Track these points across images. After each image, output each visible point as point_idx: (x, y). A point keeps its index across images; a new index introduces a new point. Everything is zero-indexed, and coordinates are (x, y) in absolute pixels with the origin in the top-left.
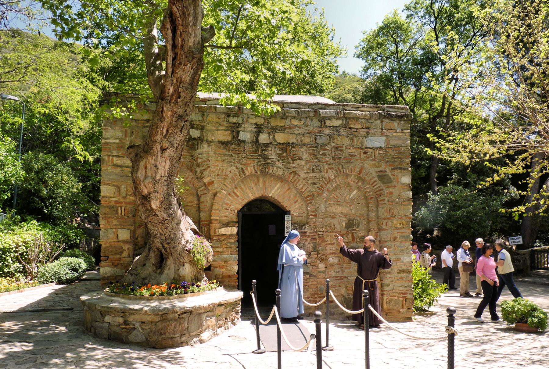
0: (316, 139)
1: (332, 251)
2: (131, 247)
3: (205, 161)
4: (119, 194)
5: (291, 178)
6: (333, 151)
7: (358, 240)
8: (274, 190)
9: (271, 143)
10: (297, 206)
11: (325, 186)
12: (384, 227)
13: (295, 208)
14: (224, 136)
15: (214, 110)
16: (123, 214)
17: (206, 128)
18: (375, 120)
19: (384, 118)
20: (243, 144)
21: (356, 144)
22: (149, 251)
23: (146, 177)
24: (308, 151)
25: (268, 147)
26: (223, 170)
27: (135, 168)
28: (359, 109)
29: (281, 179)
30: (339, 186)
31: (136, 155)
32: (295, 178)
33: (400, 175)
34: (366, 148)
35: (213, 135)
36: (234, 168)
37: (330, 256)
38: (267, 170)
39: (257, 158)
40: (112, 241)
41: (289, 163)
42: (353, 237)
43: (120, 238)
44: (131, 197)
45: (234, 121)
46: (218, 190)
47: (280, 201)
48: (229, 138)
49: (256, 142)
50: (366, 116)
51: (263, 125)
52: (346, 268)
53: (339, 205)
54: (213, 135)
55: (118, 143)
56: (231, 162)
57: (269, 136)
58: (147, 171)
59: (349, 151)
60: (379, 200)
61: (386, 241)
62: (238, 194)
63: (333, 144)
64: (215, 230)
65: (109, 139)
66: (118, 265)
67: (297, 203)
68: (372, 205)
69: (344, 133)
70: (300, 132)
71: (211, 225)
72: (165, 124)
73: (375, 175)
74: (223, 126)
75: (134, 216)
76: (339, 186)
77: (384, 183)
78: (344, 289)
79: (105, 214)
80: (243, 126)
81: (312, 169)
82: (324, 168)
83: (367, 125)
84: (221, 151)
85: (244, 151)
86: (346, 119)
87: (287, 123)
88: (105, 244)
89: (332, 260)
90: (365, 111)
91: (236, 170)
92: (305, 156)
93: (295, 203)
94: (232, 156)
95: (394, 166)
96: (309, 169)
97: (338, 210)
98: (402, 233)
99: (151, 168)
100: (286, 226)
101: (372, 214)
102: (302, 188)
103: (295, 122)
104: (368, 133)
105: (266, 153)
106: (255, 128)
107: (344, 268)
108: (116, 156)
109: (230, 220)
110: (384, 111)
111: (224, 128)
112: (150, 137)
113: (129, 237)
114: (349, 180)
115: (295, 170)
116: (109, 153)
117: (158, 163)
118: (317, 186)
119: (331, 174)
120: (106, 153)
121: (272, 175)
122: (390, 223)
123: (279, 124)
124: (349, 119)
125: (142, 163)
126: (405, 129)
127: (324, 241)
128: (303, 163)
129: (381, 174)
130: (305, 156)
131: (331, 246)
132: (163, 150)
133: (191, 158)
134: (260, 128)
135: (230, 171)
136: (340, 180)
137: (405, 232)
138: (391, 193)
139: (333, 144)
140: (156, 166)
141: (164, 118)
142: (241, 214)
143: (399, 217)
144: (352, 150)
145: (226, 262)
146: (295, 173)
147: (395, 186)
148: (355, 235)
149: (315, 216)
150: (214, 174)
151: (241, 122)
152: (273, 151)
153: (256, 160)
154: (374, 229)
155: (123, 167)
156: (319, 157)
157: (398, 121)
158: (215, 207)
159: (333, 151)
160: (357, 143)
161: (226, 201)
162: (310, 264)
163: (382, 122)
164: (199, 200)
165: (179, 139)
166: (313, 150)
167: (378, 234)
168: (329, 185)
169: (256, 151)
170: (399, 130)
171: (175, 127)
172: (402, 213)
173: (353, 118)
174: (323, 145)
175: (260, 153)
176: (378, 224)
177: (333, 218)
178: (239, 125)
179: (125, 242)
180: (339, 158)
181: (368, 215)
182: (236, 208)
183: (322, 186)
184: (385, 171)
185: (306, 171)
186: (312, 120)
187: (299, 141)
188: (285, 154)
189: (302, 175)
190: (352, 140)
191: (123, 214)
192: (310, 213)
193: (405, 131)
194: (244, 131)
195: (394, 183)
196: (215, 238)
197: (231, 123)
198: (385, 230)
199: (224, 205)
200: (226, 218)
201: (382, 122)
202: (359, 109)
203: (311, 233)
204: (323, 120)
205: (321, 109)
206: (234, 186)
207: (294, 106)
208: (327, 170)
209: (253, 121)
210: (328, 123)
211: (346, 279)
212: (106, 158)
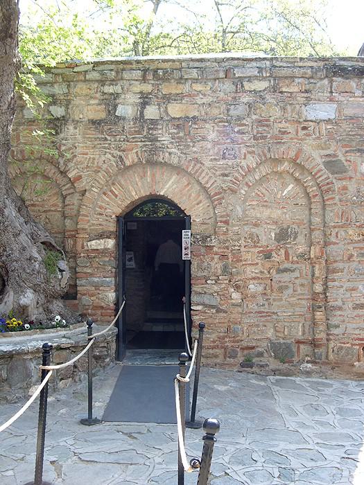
0: (228, 110)
1: (254, 275)
7: (295, 259)
8: (167, 186)
12: (333, 239)
13: (197, 211)
14: (93, 110)
17: (72, 102)
18: (321, 79)
19: (333, 76)
20: (122, 121)
21: (290, 115)
24: (216, 128)
26: (94, 159)
28: (296, 64)
29: (178, 169)
32: (197, 168)
34: (306, 121)
37: (251, 282)
38: (155, 157)
39: (141, 141)
42: (287, 254)
45: (111, 91)
46: (87, 188)
47: (176, 201)
48: (103, 115)
49: (140, 118)
51: (150, 94)
52: (274, 300)
56: (105, 148)
57: (159, 108)
59: (280, 125)
61: (335, 261)
62: (117, 193)
63: (254, 117)
64: (83, 244)
67: (201, 205)
70: (204, 101)
73: (319, 161)
74: (95, 98)
78: (272, 330)
80: (123, 96)
81: (222, 153)
82: (240, 152)
83: (308, 87)
84: (92, 133)
85: (123, 131)
87: (186, 88)
89: (253, 287)
91: (112, 158)
92: (212, 136)
93: (198, 204)
94: (106, 139)
95: (351, 147)
101: (317, 220)
103: (198, 87)
106: (140, 98)
107: (271, 300)
111: (97, 101)
115: (196, 156)
118: (229, 178)
122: (343, 233)
123: (174, 92)
127: (241, 261)
128: (209, 146)
130: (212, 136)
131: (253, 267)
133: (53, 144)
135: (104, 161)
136: (264, 170)
138: (345, 188)
139: (254, 117)
144: (283, 125)
145: (97, 287)
146: (197, 160)
147: (351, 178)
148: (290, 252)
149: (226, 222)
150: (82, 166)
151: (120, 91)
152: (164, 130)
156: (232, 135)
162: (217, 292)
163: (331, 82)
166: (224, 126)
169: (139, 132)
174: (239, 118)
175: (145, 134)
177: (256, 225)
178: (116, 96)
180: (264, 138)
182: (114, 213)
184: (335, 156)
185: (213, 157)
186: (223, 83)
188: (181, 134)
189: (208, 163)
190: (284, 109)
195: (350, 173)
196: (82, 255)
198: (335, 244)
200: (100, 227)
201: (331, 82)
202: (296, 64)
203: (219, 248)
207: (197, 65)
208: (245, 156)
209: (138, 87)
210: (247, 86)
211: (274, 317)
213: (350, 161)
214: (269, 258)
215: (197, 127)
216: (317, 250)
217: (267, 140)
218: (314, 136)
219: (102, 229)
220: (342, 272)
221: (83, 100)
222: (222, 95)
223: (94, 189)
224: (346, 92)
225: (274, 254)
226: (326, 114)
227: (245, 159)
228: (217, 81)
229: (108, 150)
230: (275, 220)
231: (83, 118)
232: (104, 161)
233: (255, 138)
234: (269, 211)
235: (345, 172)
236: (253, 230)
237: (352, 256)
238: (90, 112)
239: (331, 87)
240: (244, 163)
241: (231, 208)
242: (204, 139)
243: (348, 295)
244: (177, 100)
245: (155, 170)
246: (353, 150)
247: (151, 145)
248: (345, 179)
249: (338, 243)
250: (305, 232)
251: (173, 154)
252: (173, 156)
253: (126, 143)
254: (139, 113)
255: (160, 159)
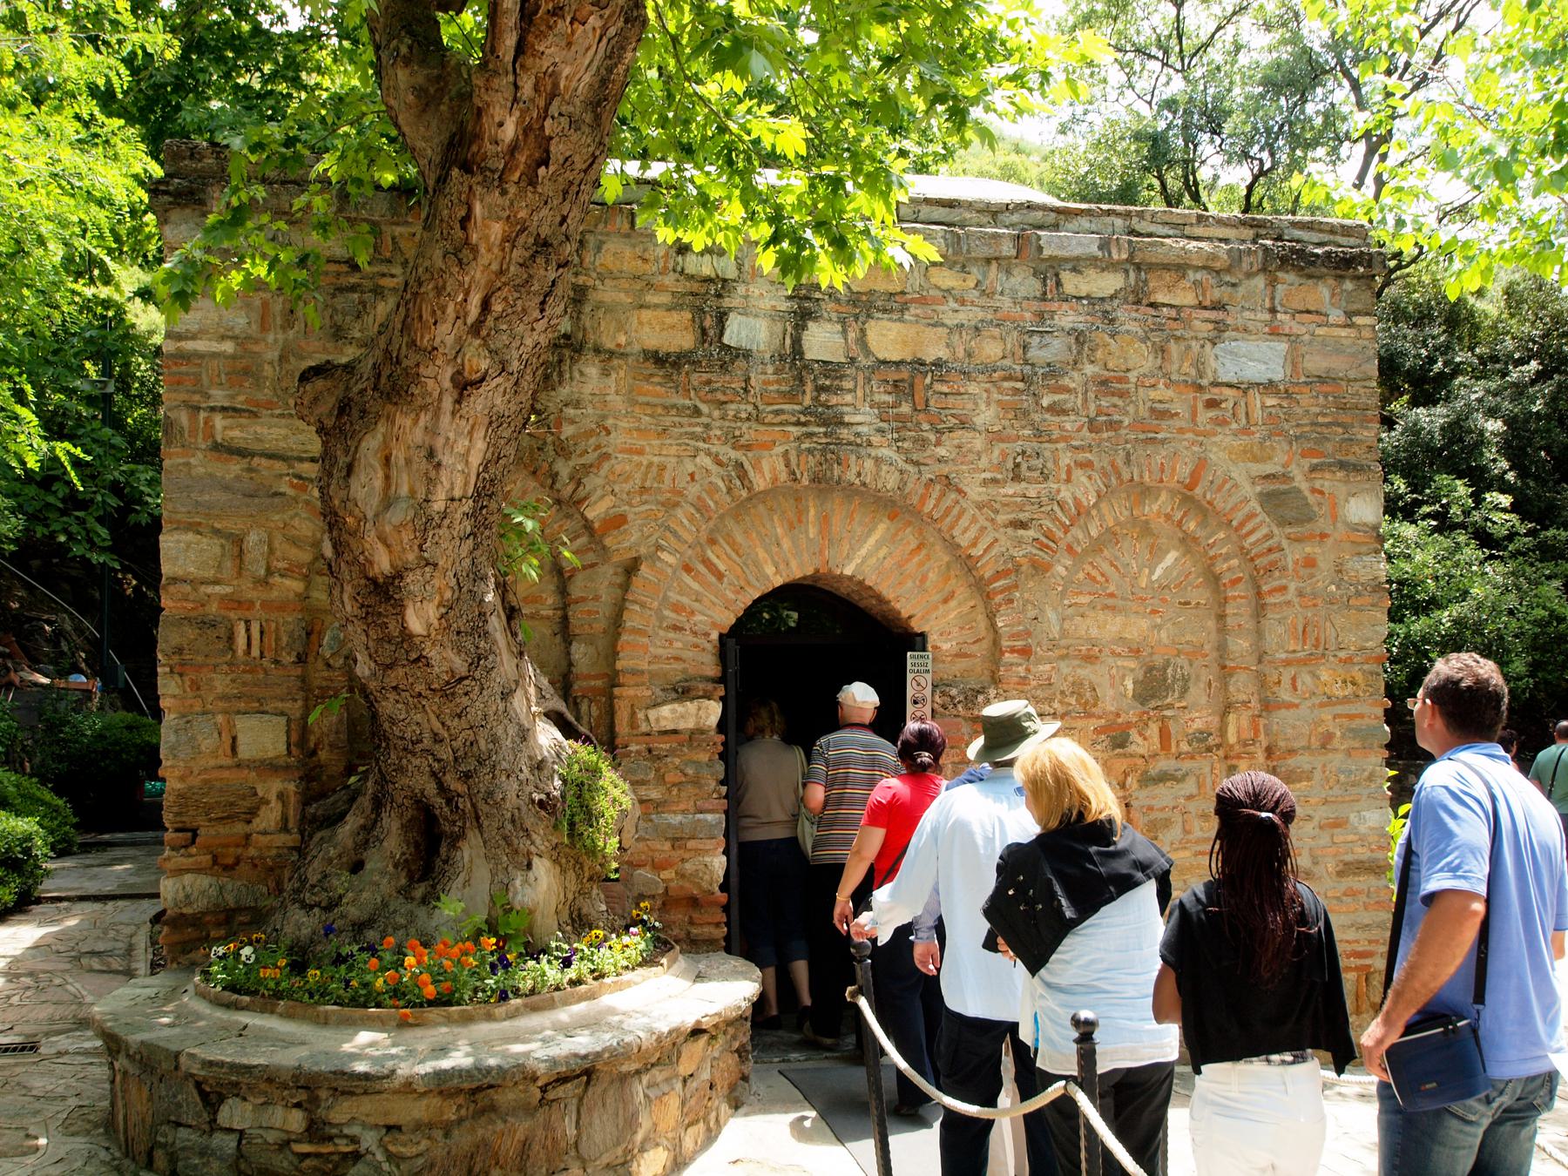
0: (1025, 347)
2: (292, 787)
3: (589, 434)
4: (240, 570)
5: (931, 503)
6: (1091, 395)
7: (1185, 747)
8: (863, 552)
9: (853, 360)
10: (953, 612)
11: (1059, 534)
12: (1285, 695)
15: (627, 226)
16: (255, 652)
17: (593, 297)
18: (1249, 275)
19: (1280, 268)
21: (1175, 367)
22: (378, 805)
23: (388, 502)
24: (996, 396)
25: (841, 378)
26: (662, 468)
27: (336, 464)
28: (1188, 231)
29: (892, 507)
30: (1111, 536)
31: (344, 408)
32: (948, 501)
33: (1342, 490)
34: (1215, 384)
35: (620, 327)
36: (707, 462)
38: (837, 470)
39: (798, 423)
40: (212, 763)
41: (923, 443)
42: (1164, 735)
43: (245, 752)
44: (288, 582)
46: (643, 551)
47: (887, 592)
50: (1213, 257)
53: (1113, 608)
54: (620, 327)
55: (233, 357)
56: (694, 436)
58: (394, 473)
59: (1153, 394)
60: (1265, 588)
61: (1292, 752)
62: (722, 567)
63: (1089, 369)
64: (633, 714)
65: (194, 337)
66: (238, 861)
67: (953, 603)
68: (1240, 612)
69: (1133, 327)
70: (962, 317)
71: (616, 691)
72: (478, 274)
73: (1248, 490)
74: (661, 289)
75: (301, 659)
76: (1111, 536)
77: (1283, 522)
79: (179, 650)
80: (741, 289)
81: (1010, 465)
82: (1056, 462)
83: (1216, 294)
84: (656, 390)
85: (745, 390)
86: (1138, 267)
88: (182, 779)
90: (1209, 239)
91: (714, 468)
92: (985, 416)
93: (945, 601)
94: (697, 412)
96: (999, 466)
97: (1106, 627)
98: (1351, 717)
99: (408, 462)
100: (910, 693)
101: (1240, 645)
102: (974, 544)
104: (1220, 328)
105: (834, 400)
108: (224, 409)
109: (692, 671)
110: (1279, 238)
111: (665, 298)
112: (405, 327)
113: (282, 748)
114: (1151, 509)
115: (945, 469)
116: (197, 397)
117: (439, 443)
118: (1031, 533)
119: (1084, 488)
120: (183, 396)
121: (852, 492)
122: (1308, 679)
124: (1151, 267)
125: (371, 444)
126: (1358, 313)
128: (979, 443)
129: (1271, 486)
130: (985, 416)
132: (464, 386)
134: (808, 298)
136: (1115, 512)
137: (1362, 716)
138: (1310, 562)
139: (1089, 369)
140: (431, 454)
141: (475, 250)
142: (731, 642)
143: (1342, 654)
144: (1162, 392)
146: (948, 482)
147: (1323, 536)
148: (1173, 727)
149: (1025, 652)
150: (627, 487)
151: (731, 273)
152: (860, 393)
153: (795, 431)
154: (1245, 703)
155: (253, 455)
156: (1036, 417)
157: (1331, 281)
158: (632, 620)
159: (1091, 395)
160: (1180, 366)
161: (674, 596)
163: (1272, 283)
164: (563, 591)
165: (529, 342)
166: (1016, 391)
167: (1262, 722)
168: (1077, 532)
169: (791, 396)
170: (1336, 316)
171: (517, 288)
172: (1351, 639)
173: (1166, 267)
174: (1053, 371)
175: (807, 401)
176: (1262, 681)
177: (1089, 659)
179: (269, 767)
180: (1113, 425)
181: (1222, 648)
182: (714, 625)
183: (1049, 535)
184: (1286, 477)
185: (988, 475)
186: (1008, 272)
187: (961, 353)
188: (906, 408)
189: (975, 492)
190: (1162, 350)
191: (255, 652)
192: (1005, 643)
193: (1359, 320)
194: (745, 312)
195: (1322, 524)
196: (633, 748)
197: (691, 277)
198: (1290, 706)
199: (666, 613)
200: (678, 666)
201: (1272, 283)
204: (1050, 271)
205: (1040, 227)
206: (703, 537)
207: (940, 213)
208: (1069, 472)
210: (1071, 283)
212: (183, 418)
213: (1322, 493)
214: (1122, 745)
215: (945, 389)
216: (1245, 723)
217: (1123, 432)
218: (1234, 426)
219: (684, 671)
220: (1309, 779)
221: (627, 292)
222: (1006, 303)
223: (664, 556)
224: (1308, 312)
225: (1134, 735)
226: (1264, 367)
227: (1068, 480)
228: (994, 265)
229: (701, 445)
230: (1135, 646)
231: (629, 344)
232: (692, 475)
233: (1093, 426)
234: (1119, 619)
235: (1310, 520)
236: (1082, 672)
237: (1328, 738)
238: (647, 329)
239: (1273, 299)
240: (1065, 494)
241: (1031, 614)
242: (964, 424)
243: (1324, 840)
244: (891, 311)
245: (829, 505)
246: (1330, 465)
247: (825, 434)
248: (1311, 537)
249: (1297, 706)
250: (1206, 675)
251: (881, 463)
252: (885, 468)
253: (754, 425)
254: (788, 341)
255: (851, 476)
